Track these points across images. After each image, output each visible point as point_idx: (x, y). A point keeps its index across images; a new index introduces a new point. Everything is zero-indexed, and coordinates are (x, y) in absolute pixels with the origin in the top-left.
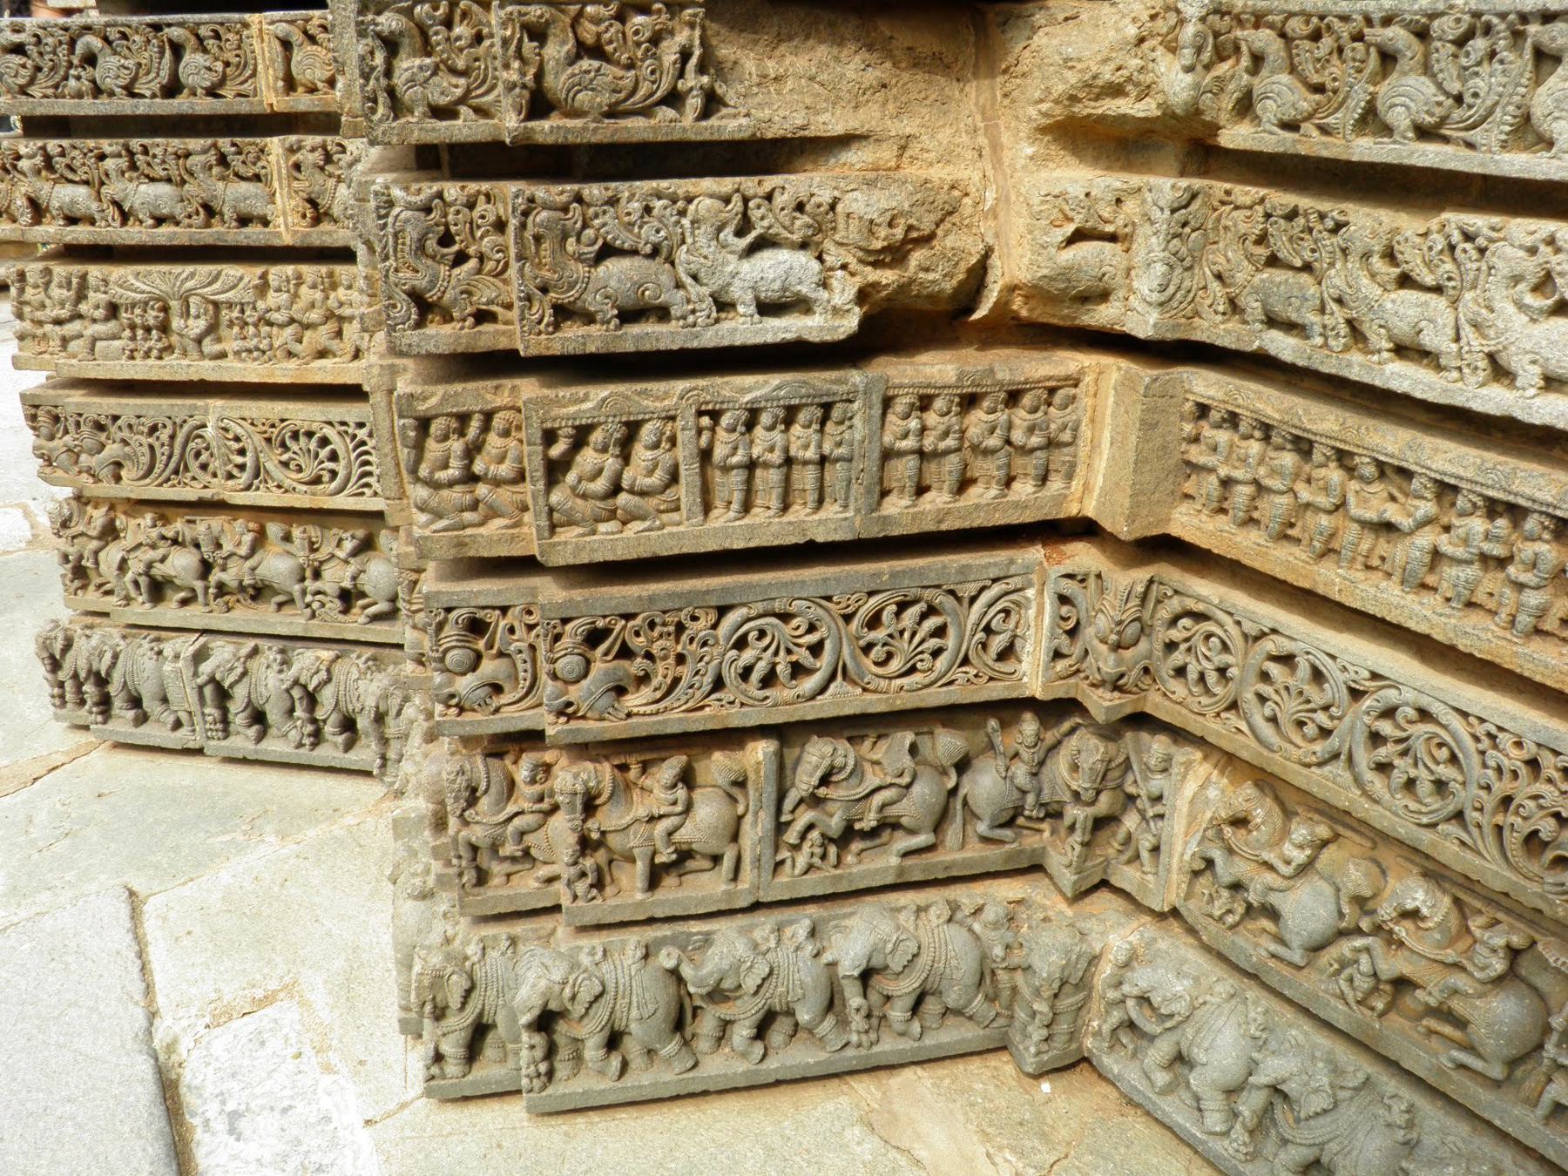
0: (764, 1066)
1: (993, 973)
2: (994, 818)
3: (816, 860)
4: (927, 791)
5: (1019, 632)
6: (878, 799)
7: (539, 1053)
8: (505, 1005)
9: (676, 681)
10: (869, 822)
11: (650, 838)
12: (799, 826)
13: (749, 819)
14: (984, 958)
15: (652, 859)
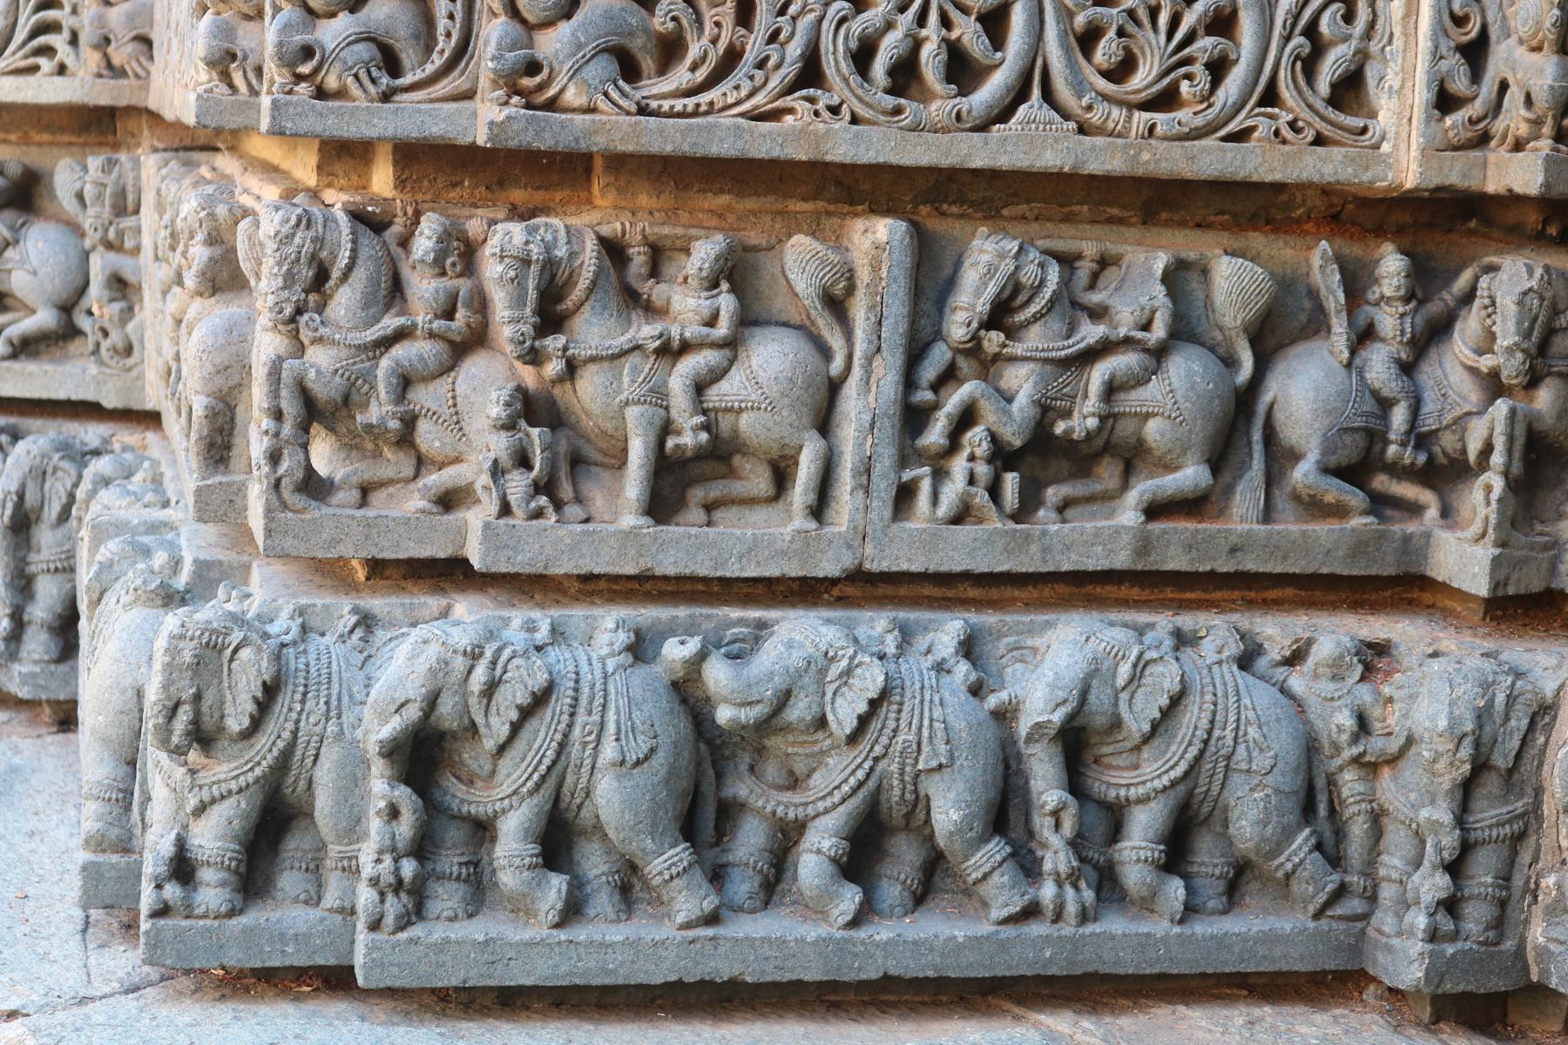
0: (862, 934)
1: (1331, 782)
2: (1328, 449)
3: (981, 497)
4: (1197, 367)
5: (1374, 47)
6: (1099, 374)
7: (405, 828)
8: (340, 735)
9: (732, 57)
10: (1082, 420)
11: (659, 396)
12: (955, 399)
13: (851, 388)
14: (1311, 748)
15: (661, 444)
